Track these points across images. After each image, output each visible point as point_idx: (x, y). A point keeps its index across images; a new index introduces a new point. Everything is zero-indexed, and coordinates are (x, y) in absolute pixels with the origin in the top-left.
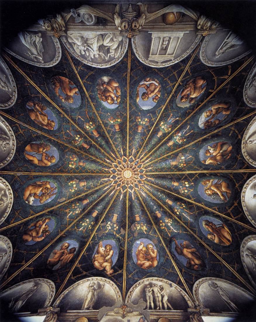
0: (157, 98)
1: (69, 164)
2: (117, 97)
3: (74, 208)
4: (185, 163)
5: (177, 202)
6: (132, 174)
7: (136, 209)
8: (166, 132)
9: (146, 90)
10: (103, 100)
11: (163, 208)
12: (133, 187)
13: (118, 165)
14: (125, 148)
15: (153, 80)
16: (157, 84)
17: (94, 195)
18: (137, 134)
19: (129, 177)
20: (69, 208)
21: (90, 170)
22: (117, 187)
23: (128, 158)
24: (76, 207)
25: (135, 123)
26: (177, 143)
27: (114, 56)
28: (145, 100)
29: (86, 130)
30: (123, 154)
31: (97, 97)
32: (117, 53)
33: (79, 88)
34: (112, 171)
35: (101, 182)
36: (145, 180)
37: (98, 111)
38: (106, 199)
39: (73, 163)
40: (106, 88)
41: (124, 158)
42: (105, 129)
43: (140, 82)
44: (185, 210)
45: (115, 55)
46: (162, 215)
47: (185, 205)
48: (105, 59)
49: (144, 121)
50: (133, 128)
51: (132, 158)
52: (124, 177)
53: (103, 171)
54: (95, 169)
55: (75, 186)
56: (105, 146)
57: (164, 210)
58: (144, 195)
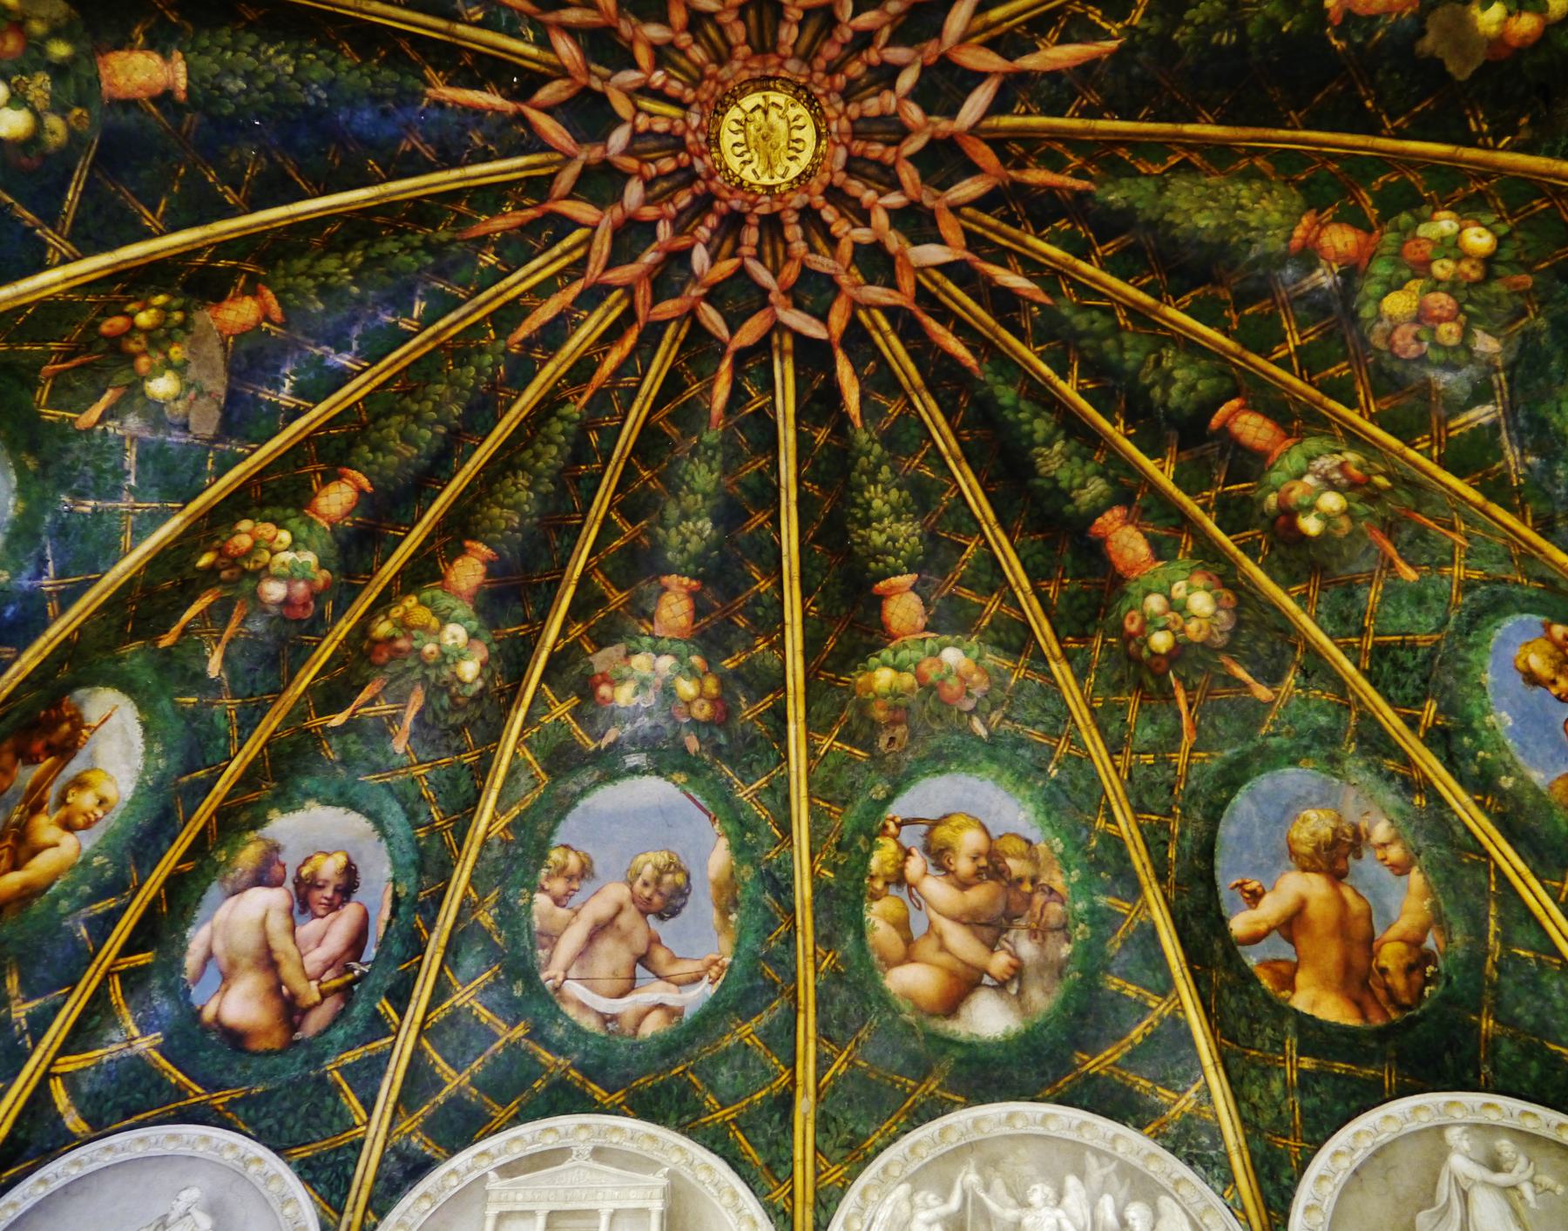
0: (559, 886)
1: (1489, 261)
2: (899, 879)
6: (714, 142)
8: (411, 602)
9: (655, 941)
10: (1029, 842)
13: (893, 241)
14: (817, 425)
15: (614, 1018)
16: (574, 989)
18: (699, 559)
19: (749, 102)
21: (1248, 176)
23: (778, 326)
25: (728, 664)
26: (279, 513)
27: (918, 1199)
28: (662, 859)
29: (1219, 576)
30: (840, 357)
31: (1075, 875)
32: (893, 1217)
33: (1217, 946)
34: (972, 170)
35: (1120, 17)
37: (1082, 761)
39: (1443, 268)
40: (991, 947)
41: (823, 318)
43: (714, 1001)
45: (905, 1207)
48: (980, 1171)
49: (643, 684)
50: (741, 622)
51: (733, 330)
52: (811, 102)
53: (1076, 162)
54: (1180, 183)
56: (1041, 427)
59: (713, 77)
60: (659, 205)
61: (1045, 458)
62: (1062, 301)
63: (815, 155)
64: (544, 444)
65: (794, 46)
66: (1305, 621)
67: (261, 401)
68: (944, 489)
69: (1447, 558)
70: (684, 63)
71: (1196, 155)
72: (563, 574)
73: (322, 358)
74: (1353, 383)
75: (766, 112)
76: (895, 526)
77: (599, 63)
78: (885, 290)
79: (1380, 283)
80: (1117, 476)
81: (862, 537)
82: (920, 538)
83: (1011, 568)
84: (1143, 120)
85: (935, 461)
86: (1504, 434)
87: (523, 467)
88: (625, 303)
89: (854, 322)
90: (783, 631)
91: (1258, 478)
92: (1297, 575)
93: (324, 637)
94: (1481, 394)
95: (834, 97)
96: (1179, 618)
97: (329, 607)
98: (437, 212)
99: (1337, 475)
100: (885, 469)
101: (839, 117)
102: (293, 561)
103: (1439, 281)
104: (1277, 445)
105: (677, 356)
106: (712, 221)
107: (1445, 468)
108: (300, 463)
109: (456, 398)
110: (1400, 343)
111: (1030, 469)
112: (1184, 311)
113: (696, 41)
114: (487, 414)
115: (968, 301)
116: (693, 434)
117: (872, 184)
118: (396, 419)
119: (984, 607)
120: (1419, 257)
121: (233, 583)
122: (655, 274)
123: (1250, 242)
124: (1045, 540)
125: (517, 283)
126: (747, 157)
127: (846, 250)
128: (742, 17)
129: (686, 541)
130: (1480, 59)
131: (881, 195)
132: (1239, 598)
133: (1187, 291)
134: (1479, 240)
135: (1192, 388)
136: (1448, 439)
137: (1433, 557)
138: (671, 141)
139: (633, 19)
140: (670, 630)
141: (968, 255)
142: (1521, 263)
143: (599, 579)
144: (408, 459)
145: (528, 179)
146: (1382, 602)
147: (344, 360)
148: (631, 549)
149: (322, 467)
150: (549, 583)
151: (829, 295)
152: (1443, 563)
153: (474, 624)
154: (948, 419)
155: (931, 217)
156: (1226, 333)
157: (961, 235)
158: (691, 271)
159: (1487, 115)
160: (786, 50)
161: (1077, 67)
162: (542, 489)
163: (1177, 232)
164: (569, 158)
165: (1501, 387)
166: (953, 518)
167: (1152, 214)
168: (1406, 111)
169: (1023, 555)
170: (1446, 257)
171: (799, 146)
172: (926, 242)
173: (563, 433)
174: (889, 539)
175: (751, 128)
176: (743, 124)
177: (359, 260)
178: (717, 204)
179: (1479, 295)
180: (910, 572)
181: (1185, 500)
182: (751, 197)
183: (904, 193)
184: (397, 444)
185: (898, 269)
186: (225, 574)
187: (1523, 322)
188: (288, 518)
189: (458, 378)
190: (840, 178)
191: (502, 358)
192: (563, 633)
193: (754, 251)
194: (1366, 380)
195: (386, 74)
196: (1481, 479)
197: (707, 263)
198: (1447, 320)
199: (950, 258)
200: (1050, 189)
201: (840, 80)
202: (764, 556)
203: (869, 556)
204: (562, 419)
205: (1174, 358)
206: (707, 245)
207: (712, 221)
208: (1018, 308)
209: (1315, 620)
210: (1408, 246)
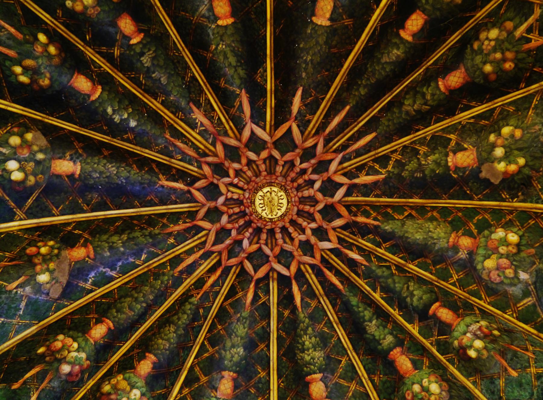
1: (518, 245)
3: (509, 55)
4: (30, 258)
5: (51, 86)
6: (253, 203)
7: (232, 51)
8: (120, 377)
11: (109, 58)
12: (247, 146)
13: (313, 240)
14: (285, 308)
17: (418, 112)
18: (238, 364)
19: (265, 190)
20: (529, 51)
21: (432, 219)
22: (315, 146)
23: (272, 269)
24: (498, 55)
26: (75, 334)
29: (441, 376)
30: (294, 282)
34: (340, 216)
36: (198, 179)
38: (363, 91)
39: (503, 250)
41: (288, 268)
42: (369, 387)
44: (11, 53)
46: (114, 25)
47: (12, 79)
50: (253, 391)
51: (256, 271)
52: (286, 191)
53: (374, 214)
54: (409, 223)
55: (499, 152)
56: (367, 314)
57: (104, 49)
58: (199, 116)
59: (254, 181)
60: (233, 224)
61: (370, 327)
62: (373, 265)
63: (287, 209)
64: (182, 314)
65: (281, 173)
66: (477, 391)
67: (79, 286)
68: (332, 337)
69: (528, 365)
70: (244, 176)
71: (414, 211)
72: (183, 366)
73: (105, 272)
74: (479, 291)
75: (271, 193)
76: (314, 353)
77: (217, 175)
78: (310, 258)
79: (482, 256)
80: (397, 334)
81: (301, 356)
82: (324, 358)
83: (359, 368)
84: (395, 198)
85: (329, 325)
86: (538, 308)
87: (173, 323)
88: (218, 258)
89: (299, 270)
90: (269, 393)
91: (450, 334)
92: (471, 373)
93: (81, 388)
94: (526, 294)
95: (293, 190)
96: (427, 395)
97: (86, 376)
98: (156, 222)
99: (479, 333)
100: (310, 329)
102: (76, 357)
103: (502, 255)
104: (455, 321)
105: (235, 279)
106: (250, 230)
107: (520, 321)
108: (88, 312)
109: (152, 292)
110: (493, 277)
111: (364, 331)
112: (416, 266)
113: (249, 169)
114: (163, 298)
115: (339, 262)
116: (238, 313)
118: (129, 299)
119: (349, 387)
120: (493, 246)
121: (50, 363)
122: (229, 248)
123: (435, 244)
124: (372, 358)
125: (180, 249)
126: (264, 208)
127: (297, 242)
129: (233, 357)
130: (501, 178)
131: (309, 223)
132: (450, 386)
133: (416, 260)
134: (513, 238)
135: (421, 298)
136: (518, 311)
137: (522, 365)
138: (239, 202)
139: (230, 162)
140: (223, 395)
141: (339, 246)
142: (529, 245)
143: (197, 369)
144: (130, 316)
145: (189, 211)
146: (506, 386)
147: (113, 274)
148: (211, 358)
149: (96, 316)
150: (177, 371)
151: (290, 259)
152: (526, 367)
153: (144, 390)
154: (333, 308)
155: (326, 232)
156: (432, 274)
157: (336, 238)
158: (242, 248)
159: (507, 193)
160: (278, 174)
161: (372, 183)
162: (179, 333)
163: (409, 240)
164: (203, 205)
165: (533, 291)
166: (336, 349)
167: (401, 234)
168: (481, 193)
169: (364, 364)
170: (503, 245)
171: (282, 205)
172: (324, 241)
173: (190, 309)
174: (312, 358)
175: (266, 198)
176: (263, 197)
177: (126, 238)
178: (253, 224)
179: (517, 258)
180: (320, 373)
181: (424, 340)
182: (265, 223)
183: (317, 223)
184: (127, 310)
185: (315, 250)
186: (47, 359)
187: (535, 266)
188: (78, 337)
189: (154, 285)
190: (295, 217)
191: (171, 278)
192: (180, 392)
193: (264, 242)
194: (484, 290)
195: (147, 176)
196: (534, 325)
197: (248, 245)
198: (508, 268)
199: (333, 247)
200: (366, 224)
201: (295, 184)
202: (263, 362)
203: (304, 365)
204: (190, 303)
205: (413, 286)
206: (248, 239)
207: (250, 230)
208: (357, 266)
209: (481, 392)
210: (489, 243)
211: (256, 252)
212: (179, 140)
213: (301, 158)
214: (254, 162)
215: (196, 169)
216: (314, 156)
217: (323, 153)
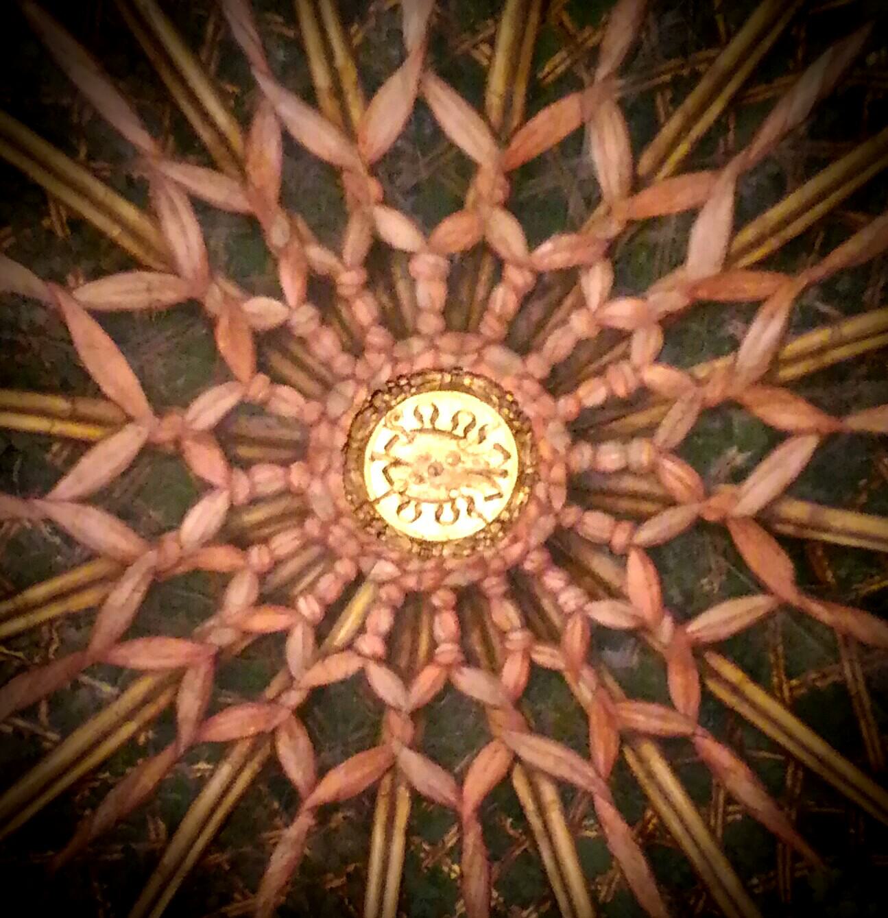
6: (426, 546)
19: (374, 484)
22: (202, 208)
23: (764, 519)
36: (273, 765)
41: (777, 437)
52: (398, 386)
59: (325, 527)
60: (507, 653)
65: (307, 396)
75: (397, 463)
77: (267, 684)
78: (756, 327)
95: (399, 352)
101: (436, 348)
113: (265, 541)
117: (559, 314)
126: (462, 505)
128: (246, 465)
131: (581, 303)
139: (212, 622)
145: (409, 832)
151: (737, 418)
157: (686, 179)
160: (311, 411)
175: (414, 490)
178: (528, 566)
183: (589, 267)
185: (722, 296)
190: (537, 365)
193: (626, 526)
197: (620, 605)
206: (593, 597)
207: (554, 580)
211: (661, 570)
212: (81, 817)
213: (251, 291)
214: (233, 510)
215: (225, 770)
216: (251, 226)
217: (244, 177)
